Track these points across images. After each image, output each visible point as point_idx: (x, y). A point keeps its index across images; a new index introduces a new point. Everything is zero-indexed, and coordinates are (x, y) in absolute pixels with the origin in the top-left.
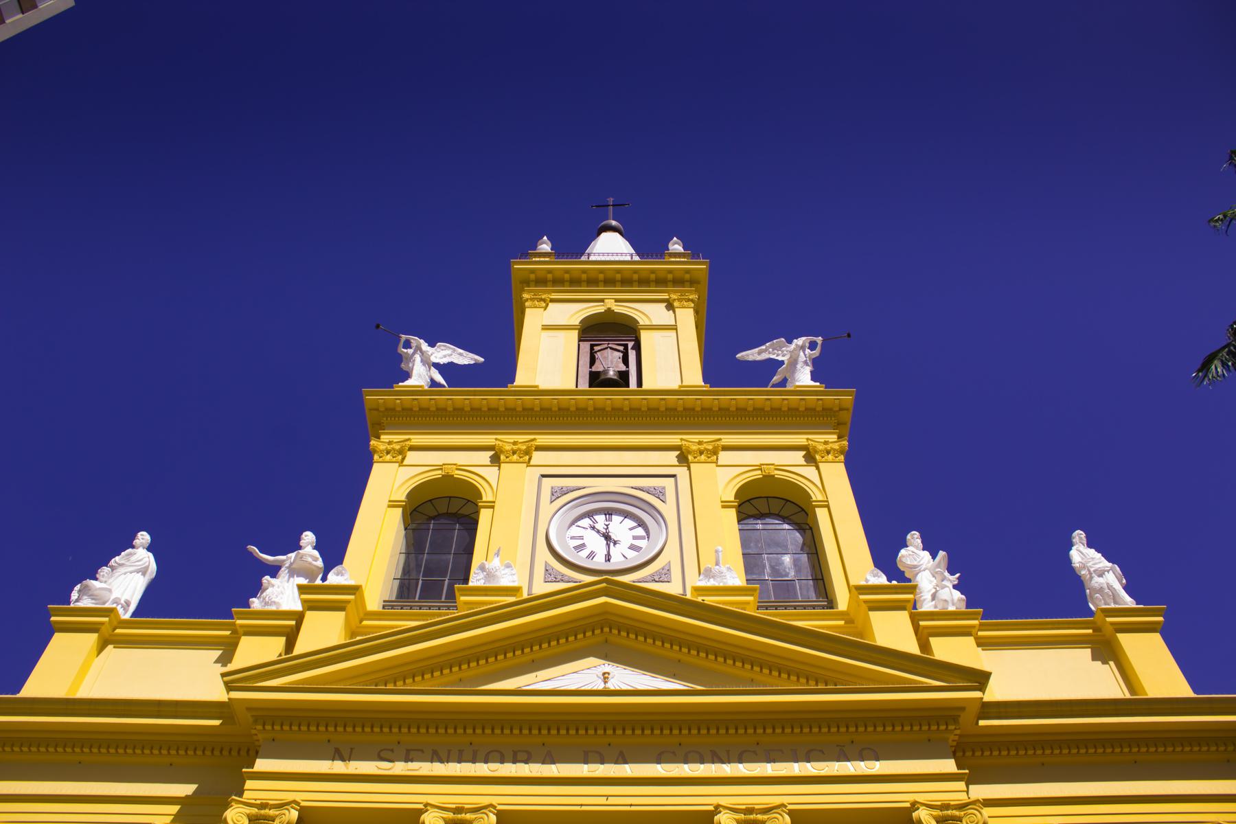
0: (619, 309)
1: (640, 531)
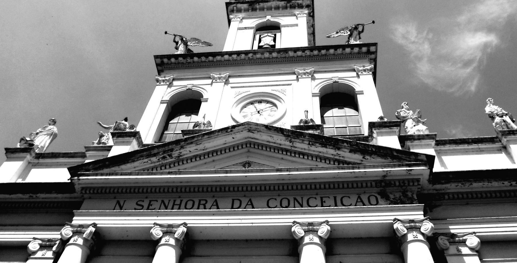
0: (272, 19)
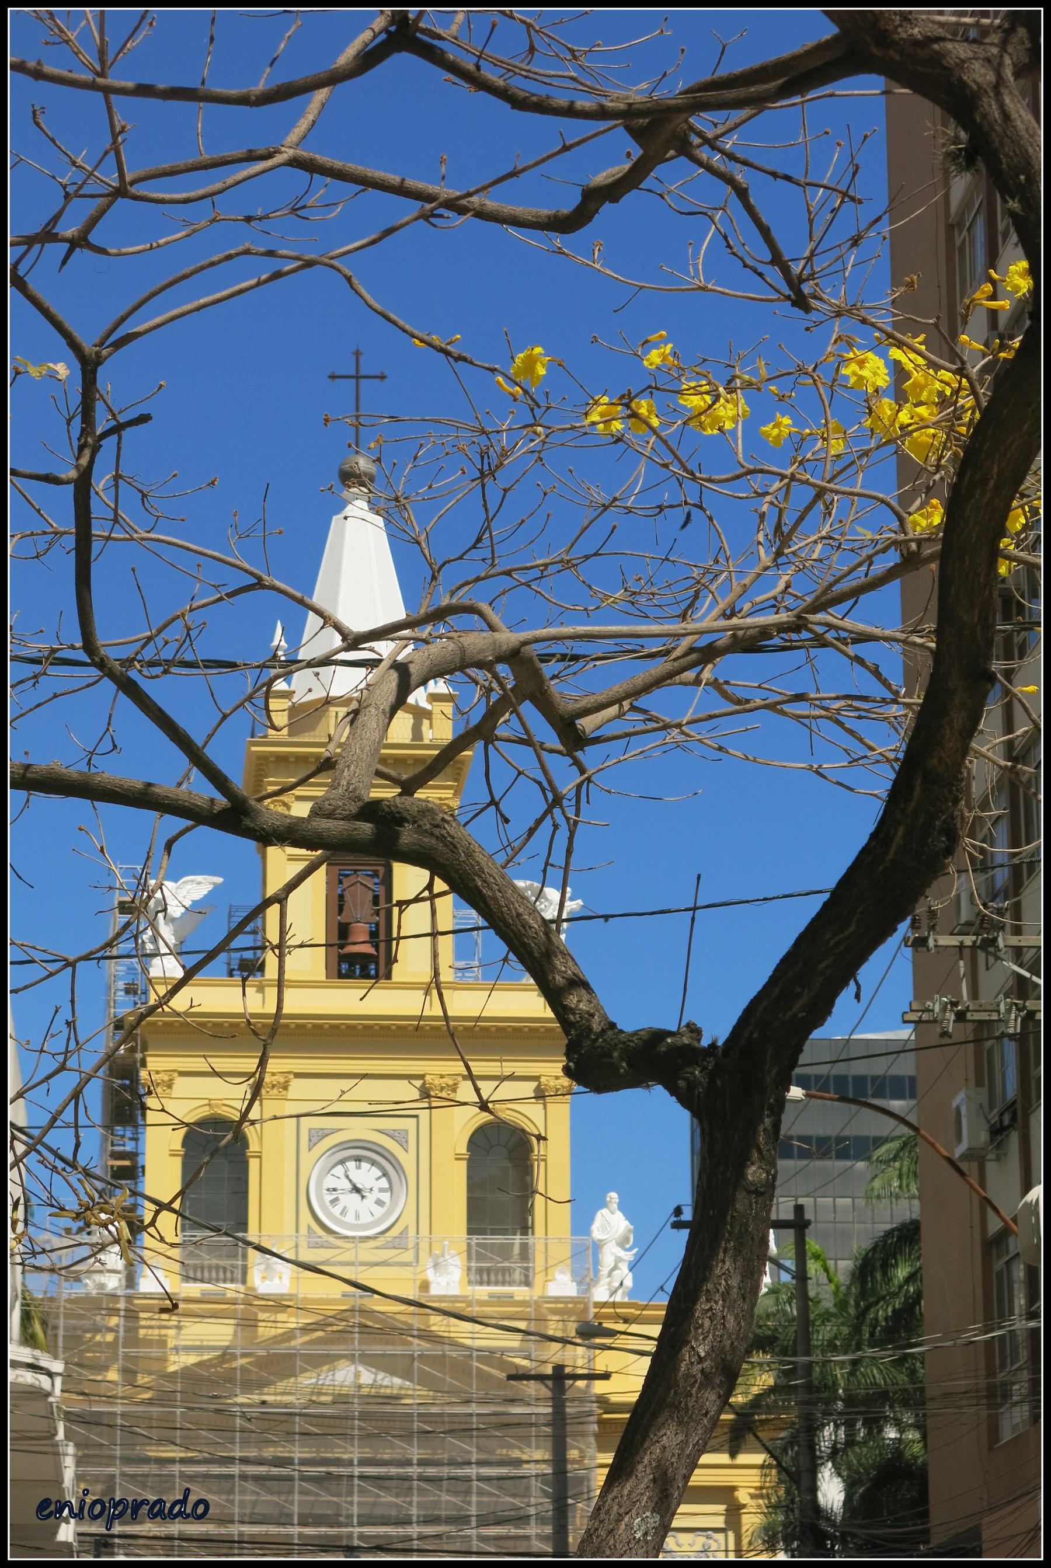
1: (384, 1183)
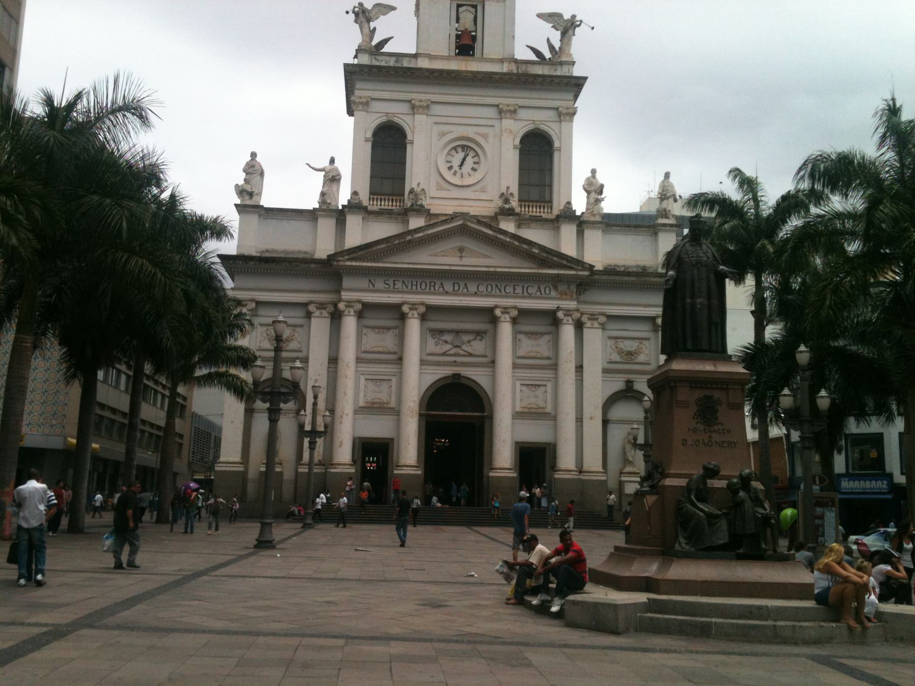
1: (476, 159)
